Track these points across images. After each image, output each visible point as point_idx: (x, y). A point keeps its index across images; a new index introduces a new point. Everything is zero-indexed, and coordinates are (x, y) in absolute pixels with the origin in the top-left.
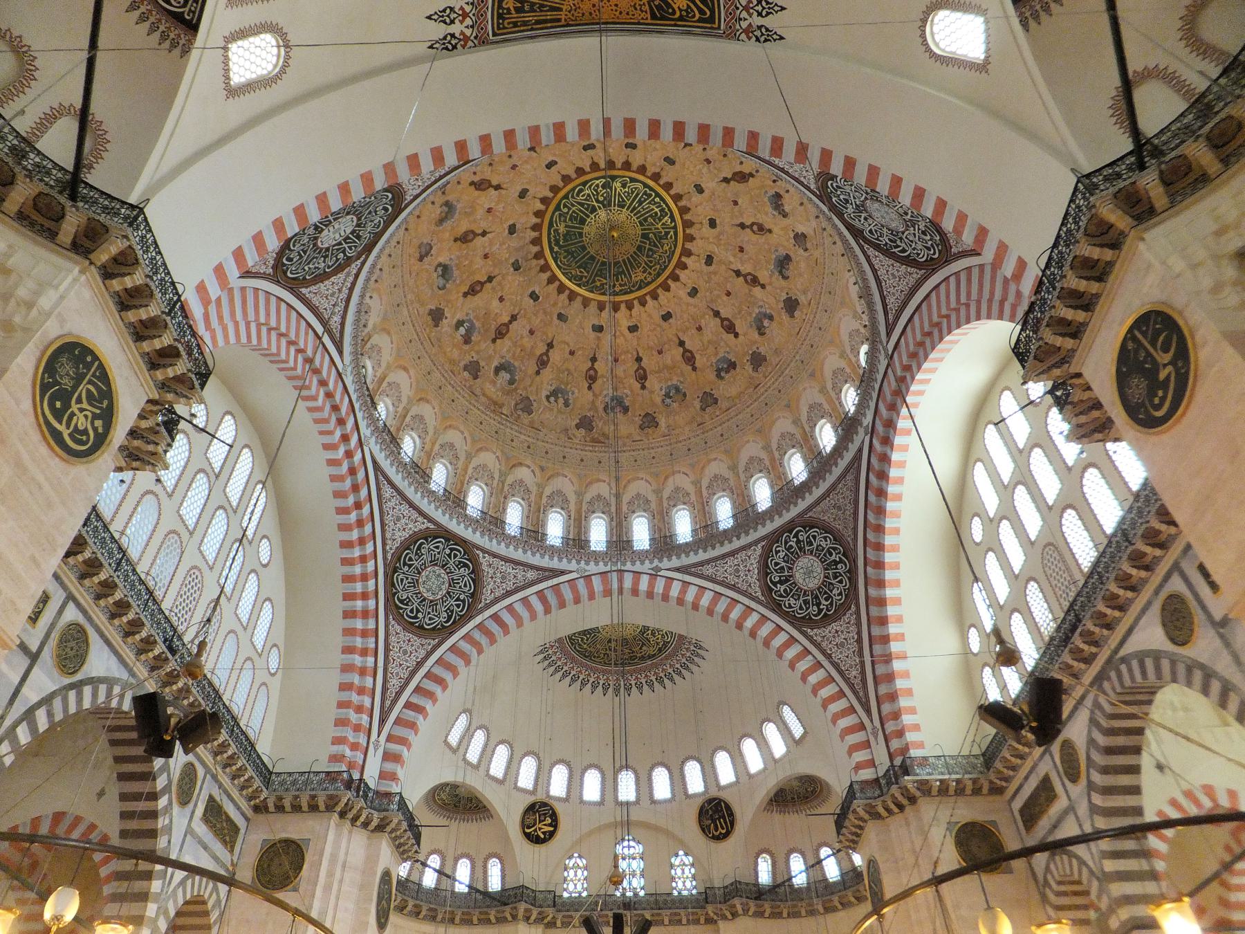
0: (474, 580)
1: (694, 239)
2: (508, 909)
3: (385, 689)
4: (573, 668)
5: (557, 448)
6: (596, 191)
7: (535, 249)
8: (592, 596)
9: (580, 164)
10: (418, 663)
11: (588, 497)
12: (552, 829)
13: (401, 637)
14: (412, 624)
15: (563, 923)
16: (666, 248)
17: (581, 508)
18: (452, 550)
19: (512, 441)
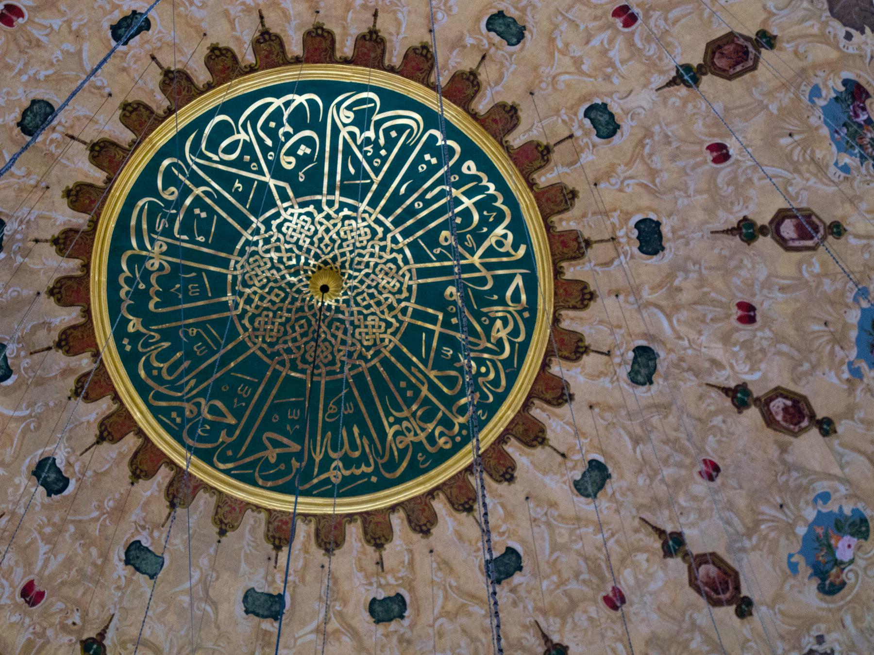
1: (592, 296)
6: (272, 134)
7: (69, 316)
9: (221, 36)
16: (500, 331)
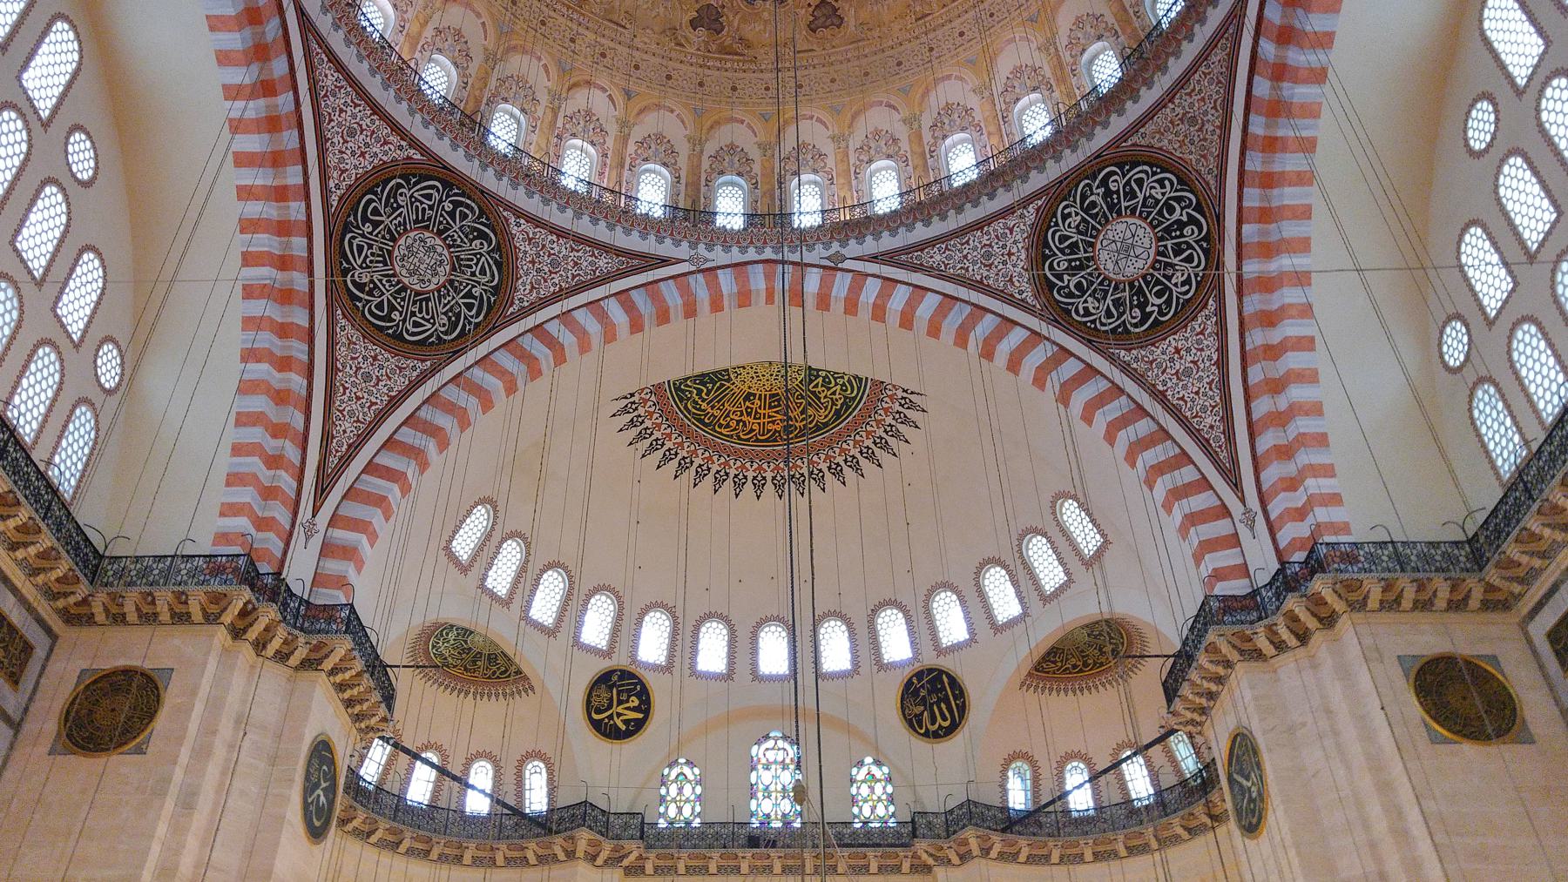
0: (499, 265)
2: (558, 845)
3: (327, 437)
4: (681, 444)
5: (653, 60)
8: (716, 306)
10: (392, 398)
11: (710, 148)
12: (641, 716)
13: (357, 349)
14: (381, 329)
15: (656, 869)
17: (699, 166)
18: (456, 204)
19: (572, 40)
